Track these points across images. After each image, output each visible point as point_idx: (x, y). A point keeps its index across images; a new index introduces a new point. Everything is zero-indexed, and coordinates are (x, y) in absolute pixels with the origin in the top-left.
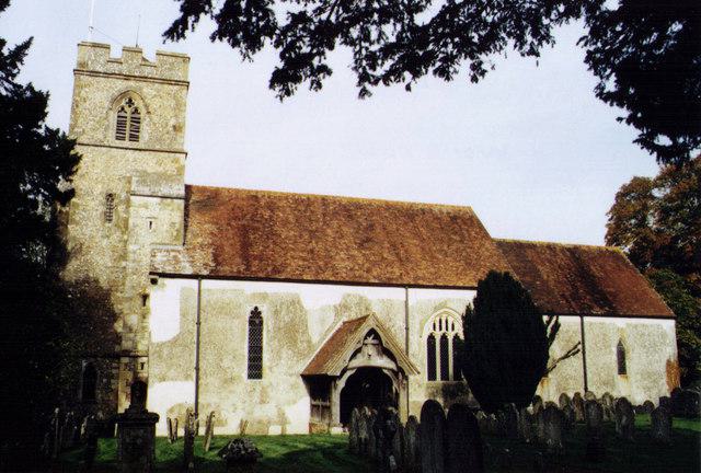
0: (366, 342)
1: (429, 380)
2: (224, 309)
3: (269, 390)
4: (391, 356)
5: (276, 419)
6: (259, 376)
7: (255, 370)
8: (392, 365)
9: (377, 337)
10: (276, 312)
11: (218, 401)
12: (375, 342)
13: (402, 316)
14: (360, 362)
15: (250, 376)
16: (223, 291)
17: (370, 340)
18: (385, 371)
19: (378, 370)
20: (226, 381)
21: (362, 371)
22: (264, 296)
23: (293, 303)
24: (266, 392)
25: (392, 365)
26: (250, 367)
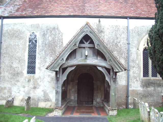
0: (82, 45)
1: (144, 76)
2: (16, 35)
3: (39, 81)
4: (103, 57)
5: (42, 98)
6: (34, 72)
7: (31, 69)
8: (103, 64)
9: (92, 42)
10: (44, 35)
11: (9, 86)
12: (91, 45)
13: (124, 36)
14: (78, 61)
15: (28, 72)
16: (15, 24)
17: (87, 44)
18: (99, 68)
19: (94, 67)
20: (14, 75)
21: (79, 67)
22: (37, 26)
23: (54, 28)
24: (37, 82)
25: (103, 64)
26: (29, 67)
